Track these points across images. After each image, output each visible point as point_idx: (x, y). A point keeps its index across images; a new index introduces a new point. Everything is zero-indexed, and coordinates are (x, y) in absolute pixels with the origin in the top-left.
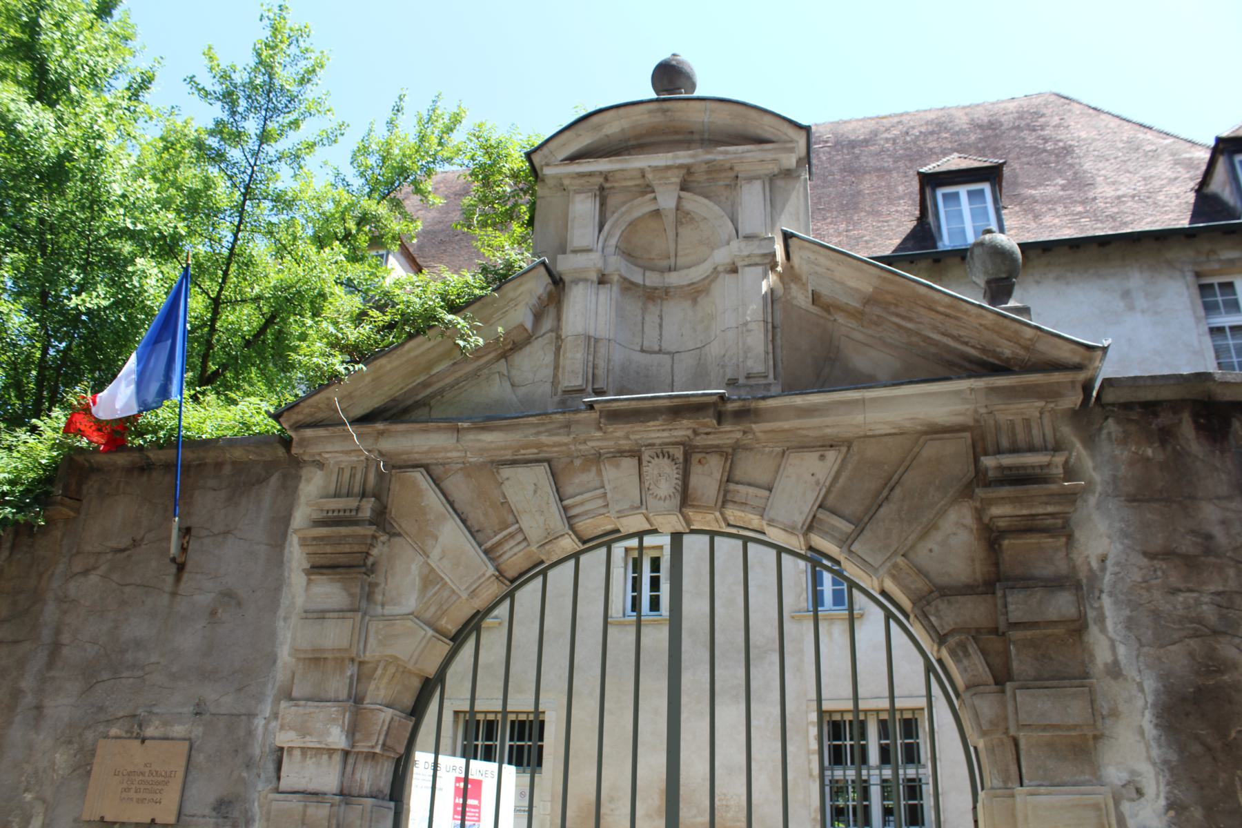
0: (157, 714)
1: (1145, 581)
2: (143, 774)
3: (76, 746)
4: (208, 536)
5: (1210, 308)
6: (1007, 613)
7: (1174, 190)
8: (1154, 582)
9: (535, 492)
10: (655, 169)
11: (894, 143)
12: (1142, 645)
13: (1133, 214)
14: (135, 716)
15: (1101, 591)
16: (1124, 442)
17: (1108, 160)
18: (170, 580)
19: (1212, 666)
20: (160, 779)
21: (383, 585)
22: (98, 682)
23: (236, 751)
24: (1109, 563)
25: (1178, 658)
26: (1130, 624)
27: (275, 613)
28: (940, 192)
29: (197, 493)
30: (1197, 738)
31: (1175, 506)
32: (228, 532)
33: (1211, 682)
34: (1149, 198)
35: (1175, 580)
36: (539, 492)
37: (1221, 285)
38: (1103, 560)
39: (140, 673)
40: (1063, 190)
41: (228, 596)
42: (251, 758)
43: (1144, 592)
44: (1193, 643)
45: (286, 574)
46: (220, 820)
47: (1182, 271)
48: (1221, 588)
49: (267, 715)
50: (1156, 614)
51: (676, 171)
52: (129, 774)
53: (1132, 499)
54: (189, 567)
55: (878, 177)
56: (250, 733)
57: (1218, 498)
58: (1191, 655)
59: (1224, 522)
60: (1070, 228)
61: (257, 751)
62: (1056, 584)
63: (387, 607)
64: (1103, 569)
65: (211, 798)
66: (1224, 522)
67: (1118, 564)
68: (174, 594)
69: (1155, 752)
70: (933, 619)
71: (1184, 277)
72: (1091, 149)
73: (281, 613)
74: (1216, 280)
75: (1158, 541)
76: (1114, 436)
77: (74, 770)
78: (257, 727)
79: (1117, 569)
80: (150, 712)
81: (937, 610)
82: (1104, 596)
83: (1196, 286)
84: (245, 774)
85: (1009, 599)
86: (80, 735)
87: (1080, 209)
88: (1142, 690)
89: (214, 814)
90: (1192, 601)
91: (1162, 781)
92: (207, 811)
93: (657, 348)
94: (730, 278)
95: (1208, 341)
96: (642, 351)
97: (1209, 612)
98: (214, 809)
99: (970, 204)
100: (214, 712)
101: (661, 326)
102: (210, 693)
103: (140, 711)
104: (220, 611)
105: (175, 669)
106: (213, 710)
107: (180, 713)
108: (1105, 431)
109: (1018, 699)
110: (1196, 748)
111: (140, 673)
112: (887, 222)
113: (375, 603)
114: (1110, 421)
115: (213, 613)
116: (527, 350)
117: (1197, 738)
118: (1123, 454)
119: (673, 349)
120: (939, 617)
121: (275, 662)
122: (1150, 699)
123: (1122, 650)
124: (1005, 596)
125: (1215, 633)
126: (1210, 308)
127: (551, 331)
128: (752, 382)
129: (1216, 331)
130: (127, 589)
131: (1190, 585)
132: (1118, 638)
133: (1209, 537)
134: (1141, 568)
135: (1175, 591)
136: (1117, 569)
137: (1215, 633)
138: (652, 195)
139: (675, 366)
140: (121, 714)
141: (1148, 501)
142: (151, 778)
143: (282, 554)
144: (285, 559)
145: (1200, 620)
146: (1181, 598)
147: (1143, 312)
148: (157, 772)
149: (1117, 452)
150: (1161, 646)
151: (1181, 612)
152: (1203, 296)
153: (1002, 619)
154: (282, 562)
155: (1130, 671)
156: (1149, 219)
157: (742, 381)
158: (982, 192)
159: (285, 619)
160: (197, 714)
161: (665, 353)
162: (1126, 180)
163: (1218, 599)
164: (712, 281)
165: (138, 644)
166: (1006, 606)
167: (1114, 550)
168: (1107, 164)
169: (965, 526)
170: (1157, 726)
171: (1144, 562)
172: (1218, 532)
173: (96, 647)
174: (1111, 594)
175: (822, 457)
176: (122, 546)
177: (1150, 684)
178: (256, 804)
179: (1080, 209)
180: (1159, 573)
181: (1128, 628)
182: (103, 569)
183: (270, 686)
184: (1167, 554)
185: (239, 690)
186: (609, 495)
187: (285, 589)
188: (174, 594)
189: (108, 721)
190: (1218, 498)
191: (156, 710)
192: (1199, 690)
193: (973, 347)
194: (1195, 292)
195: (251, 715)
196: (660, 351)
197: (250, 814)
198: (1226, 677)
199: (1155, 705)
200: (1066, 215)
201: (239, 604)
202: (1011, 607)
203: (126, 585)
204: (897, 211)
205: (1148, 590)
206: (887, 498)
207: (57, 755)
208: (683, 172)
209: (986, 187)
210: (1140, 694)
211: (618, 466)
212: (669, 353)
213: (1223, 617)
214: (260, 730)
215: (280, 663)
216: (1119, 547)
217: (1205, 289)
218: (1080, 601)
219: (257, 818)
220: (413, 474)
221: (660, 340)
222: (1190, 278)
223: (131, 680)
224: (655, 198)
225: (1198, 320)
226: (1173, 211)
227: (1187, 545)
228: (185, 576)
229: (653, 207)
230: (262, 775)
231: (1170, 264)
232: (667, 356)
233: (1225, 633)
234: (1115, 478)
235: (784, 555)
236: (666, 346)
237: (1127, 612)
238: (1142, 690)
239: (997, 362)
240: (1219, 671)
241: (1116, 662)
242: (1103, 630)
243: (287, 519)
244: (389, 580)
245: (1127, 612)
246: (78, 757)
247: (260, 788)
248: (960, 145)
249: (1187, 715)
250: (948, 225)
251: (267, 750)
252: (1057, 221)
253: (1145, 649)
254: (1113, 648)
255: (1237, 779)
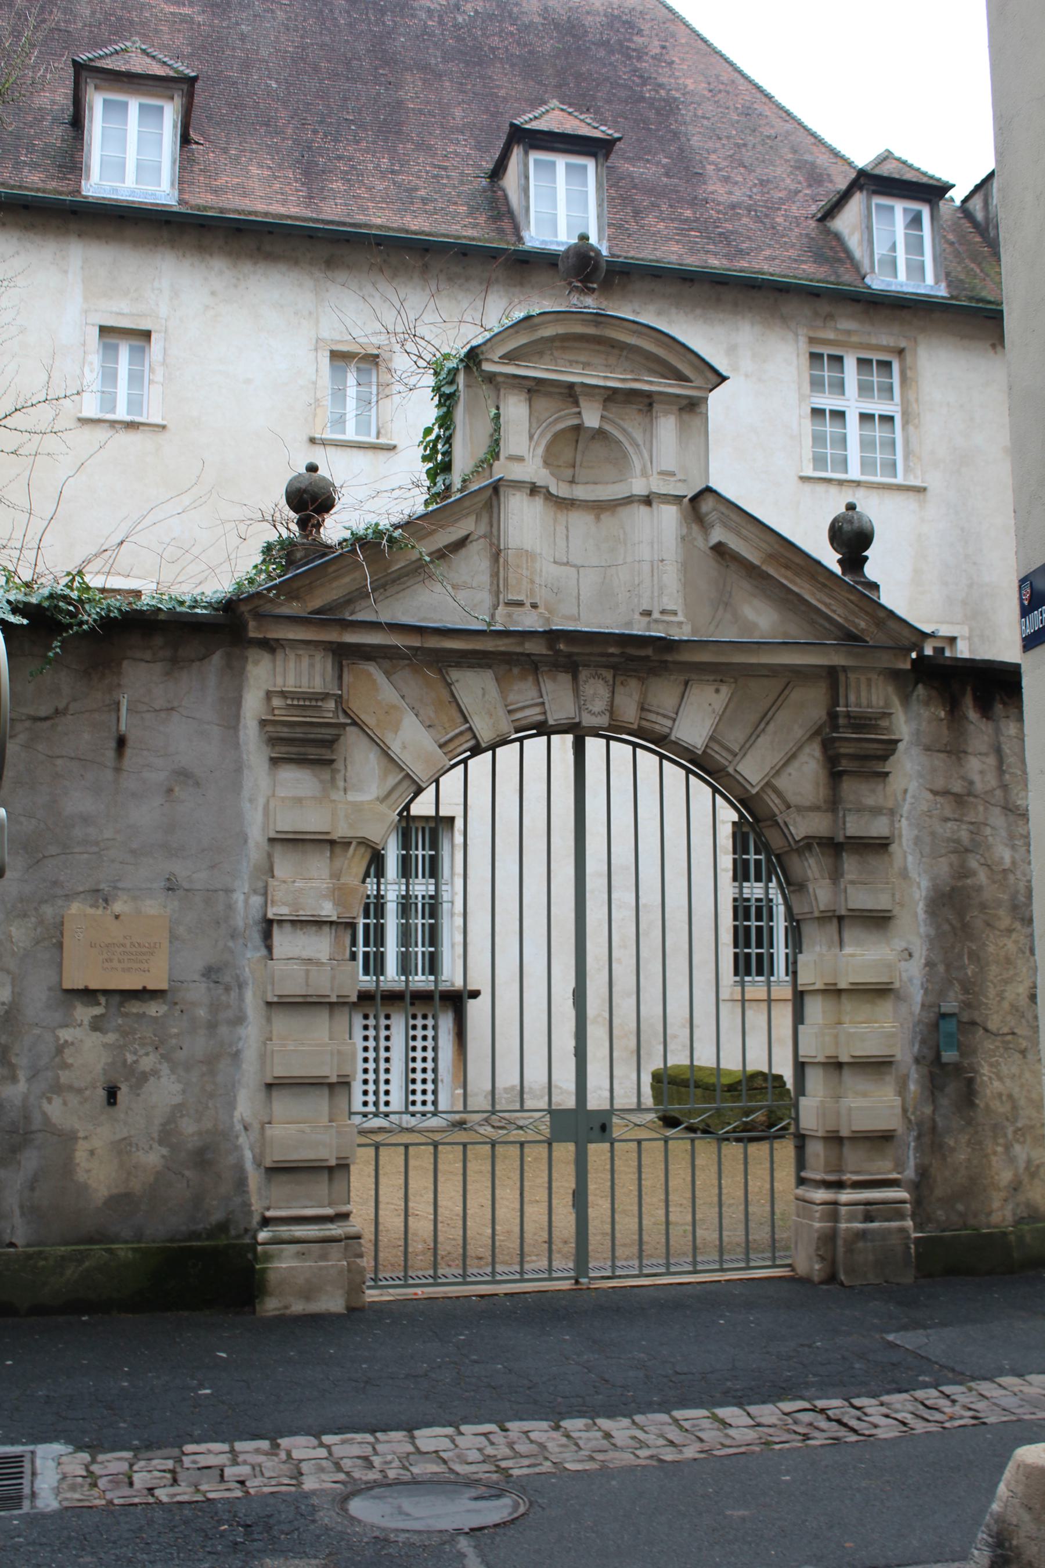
0: (123, 889)
1: (929, 811)
2: (124, 945)
3: (33, 919)
4: (148, 711)
5: (816, 384)
6: (844, 829)
7: (795, 210)
8: (935, 812)
9: (484, 695)
10: (583, 385)
11: (441, 22)
12: (922, 856)
13: (749, 238)
14: (98, 891)
15: (901, 816)
16: (927, 703)
17: (720, 139)
18: (111, 754)
19: (963, 873)
20: (144, 950)
21: (343, 772)
22: (44, 857)
23: (218, 923)
24: (909, 795)
25: (944, 867)
26: (917, 841)
27: (239, 794)
28: (534, 156)
29: (125, 664)
30: (948, 921)
31: (954, 757)
32: (172, 709)
33: (960, 884)
34: (767, 216)
35: (948, 812)
36: (487, 696)
37: (831, 357)
38: (905, 791)
39: (95, 849)
40: (667, 175)
41: (184, 775)
42: (235, 929)
43: (927, 819)
44: (953, 858)
45: (245, 757)
46: (212, 985)
47: (797, 335)
48: (974, 820)
49: (246, 891)
50: (933, 834)
51: (602, 391)
52: (107, 946)
53: (928, 749)
54: (130, 743)
55: (424, 81)
56: (230, 907)
57: (980, 754)
58: (951, 865)
59: (981, 772)
60: (678, 242)
61: (240, 922)
62: (876, 811)
63: (349, 793)
64: (904, 800)
65: (200, 965)
66: (981, 772)
67: (914, 797)
68: (118, 770)
69: (922, 930)
70: (791, 828)
71: (797, 341)
72: (700, 113)
73: (246, 793)
74: (826, 351)
75: (940, 784)
76: (921, 697)
77: (37, 943)
78: (236, 902)
79: (913, 801)
80: (115, 888)
81: (795, 822)
82: (903, 820)
83: (807, 356)
84: (231, 944)
85: (847, 819)
86: (36, 909)
87: (688, 213)
88: (919, 888)
89: (204, 979)
90: (955, 827)
91: (925, 948)
92: (196, 977)
93: (565, 560)
94: (643, 509)
95: (807, 425)
96: (555, 562)
97: (964, 835)
98: (203, 975)
99: (567, 183)
100: (186, 887)
101: (567, 537)
102: (181, 869)
103: (102, 886)
104: (177, 789)
105: (134, 846)
106: (186, 885)
107: (150, 889)
108: (915, 694)
109: (849, 891)
110: (946, 927)
111: (95, 849)
112: (445, 169)
113: (338, 789)
114: (920, 686)
115: (170, 791)
116: (463, 552)
117: (948, 921)
118: (925, 713)
119: (579, 563)
120: (796, 828)
121: (246, 841)
122: (924, 894)
123: (910, 858)
124: (844, 816)
125: (967, 850)
126: (816, 384)
127: (485, 536)
128: (666, 618)
129: (817, 413)
130: (59, 762)
131: (956, 816)
132: (909, 851)
133: (971, 783)
134: (928, 801)
135: (947, 820)
136: (913, 801)
137: (967, 850)
138: (577, 410)
139: (581, 580)
140: (81, 889)
141: (939, 751)
142: (134, 949)
143: (237, 737)
144: (241, 741)
145: (958, 841)
146: (949, 824)
147: (747, 376)
148: (139, 944)
149: (922, 711)
150: (934, 858)
151: (948, 835)
152: (812, 367)
153: (841, 833)
154: (238, 744)
155: (913, 874)
156: (768, 252)
157: (656, 615)
158: (584, 168)
159: (251, 801)
160: (169, 889)
161: (571, 566)
162: (739, 179)
163: (971, 827)
164: (621, 505)
165: (86, 820)
166: (844, 823)
167: (913, 786)
168: (718, 145)
169: (814, 757)
170: (926, 912)
171: (930, 796)
172: (976, 778)
173: (33, 821)
174: (908, 819)
175: (717, 691)
176: (42, 713)
177: (925, 883)
178: (247, 969)
179: (688, 213)
180: (939, 806)
181: (916, 844)
182: (22, 738)
183: (245, 864)
184: (946, 793)
185: (212, 867)
186: (547, 706)
187: (246, 772)
188: (118, 770)
189: (66, 896)
190: (980, 754)
191: (120, 885)
192: (953, 889)
193: (839, 615)
194: (805, 360)
195: (228, 891)
196: (567, 564)
197: (241, 979)
198: (969, 881)
199: (926, 898)
200: (672, 220)
201: (197, 784)
202: (848, 825)
203: (58, 757)
204: (457, 154)
205: (930, 817)
206: (763, 730)
207: (12, 928)
208: (610, 393)
209: (590, 164)
210: (918, 891)
211: (554, 680)
212: (574, 566)
213: (972, 840)
214: (240, 905)
215: (251, 843)
216: (916, 784)
217: (815, 358)
218: (892, 824)
219: (250, 982)
220: (366, 667)
221: (567, 552)
222: (804, 348)
223: (86, 856)
224: (579, 413)
225: (802, 398)
226: (793, 246)
227: (957, 787)
228: (128, 752)
229: (576, 422)
230: (249, 945)
231: (784, 320)
232: (573, 569)
233: (971, 851)
234: (918, 730)
235: (665, 762)
236: (573, 560)
237: (916, 832)
238: (919, 888)
239: (855, 631)
240: (966, 877)
241: (905, 868)
242: (900, 845)
243: (237, 702)
244: (349, 768)
245: (916, 832)
246: (39, 930)
247: (249, 955)
248: (530, 52)
249: (944, 905)
250: (536, 207)
251: (251, 922)
252: (661, 226)
253: (924, 860)
254: (905, 857)
255: (966, 950)
